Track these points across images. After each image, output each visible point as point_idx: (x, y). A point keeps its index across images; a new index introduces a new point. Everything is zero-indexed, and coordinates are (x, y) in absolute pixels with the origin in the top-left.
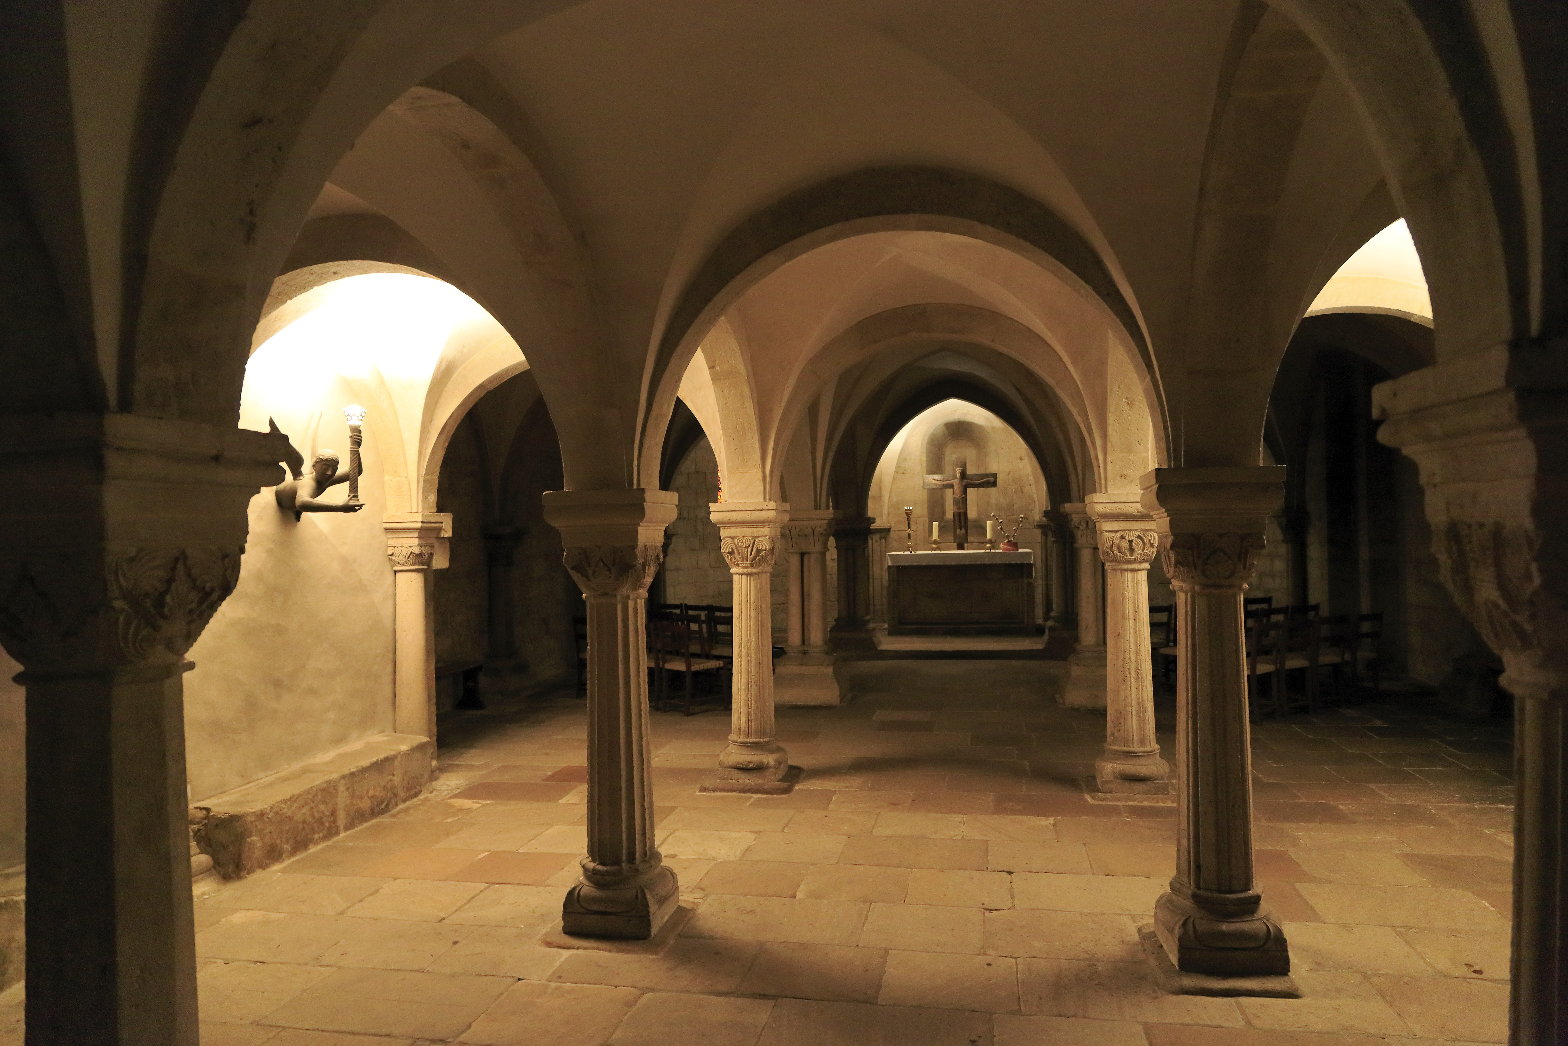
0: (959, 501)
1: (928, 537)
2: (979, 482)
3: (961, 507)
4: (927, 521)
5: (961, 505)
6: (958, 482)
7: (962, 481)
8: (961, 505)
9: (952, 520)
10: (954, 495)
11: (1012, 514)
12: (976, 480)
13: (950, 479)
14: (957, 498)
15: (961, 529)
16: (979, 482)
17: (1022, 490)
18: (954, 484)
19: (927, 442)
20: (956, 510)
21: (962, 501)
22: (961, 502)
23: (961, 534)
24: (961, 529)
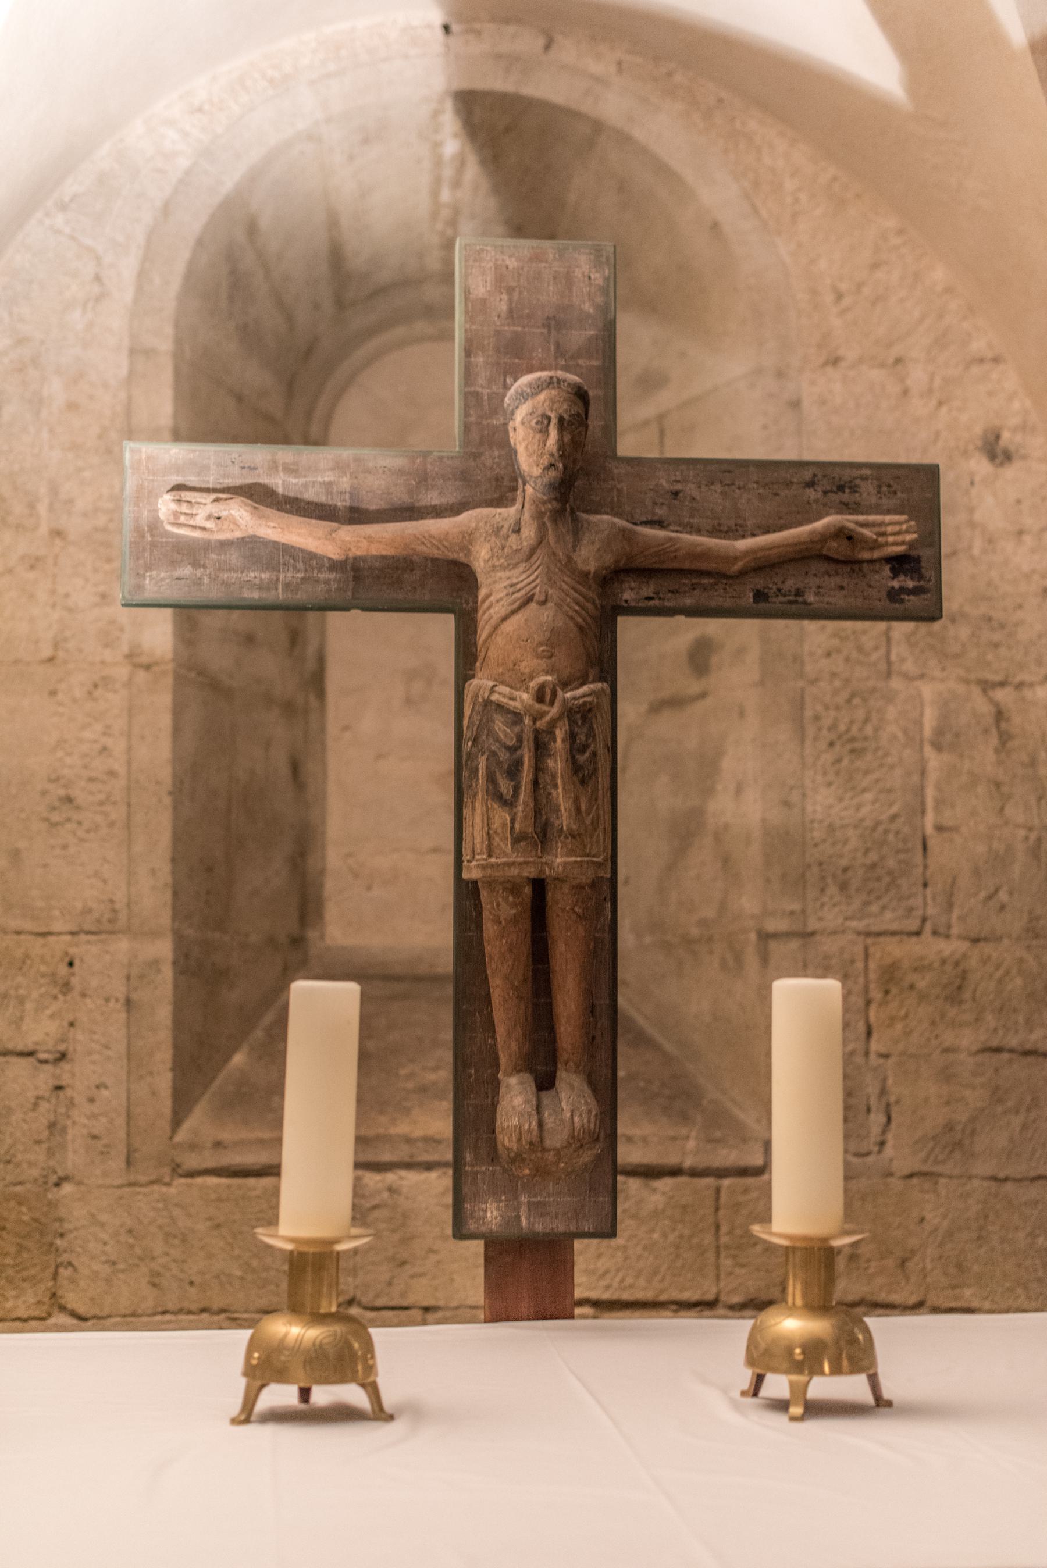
0: (541, 748)
1: (166, 1105)
2: (743, 544)
3: (565, 820)
4: (167, 973)
5: (561, 797)
6: (529, 532)
7: (577, 531)
8: (561, 797)
9: (446, 963)
10: (480, 683)
11: (913, 925)
12: (716, 531)
13: (432, 498)
14: (516, 718)
15: (545, 1083)
16: (743, 544)
17: (1000, 715)
18: (481, 557)
19: (189, 275)
20: (507, 853)
21: (575, 747)
22: (557, 764)
23: (555, 1140)
24: (545, 1083)
